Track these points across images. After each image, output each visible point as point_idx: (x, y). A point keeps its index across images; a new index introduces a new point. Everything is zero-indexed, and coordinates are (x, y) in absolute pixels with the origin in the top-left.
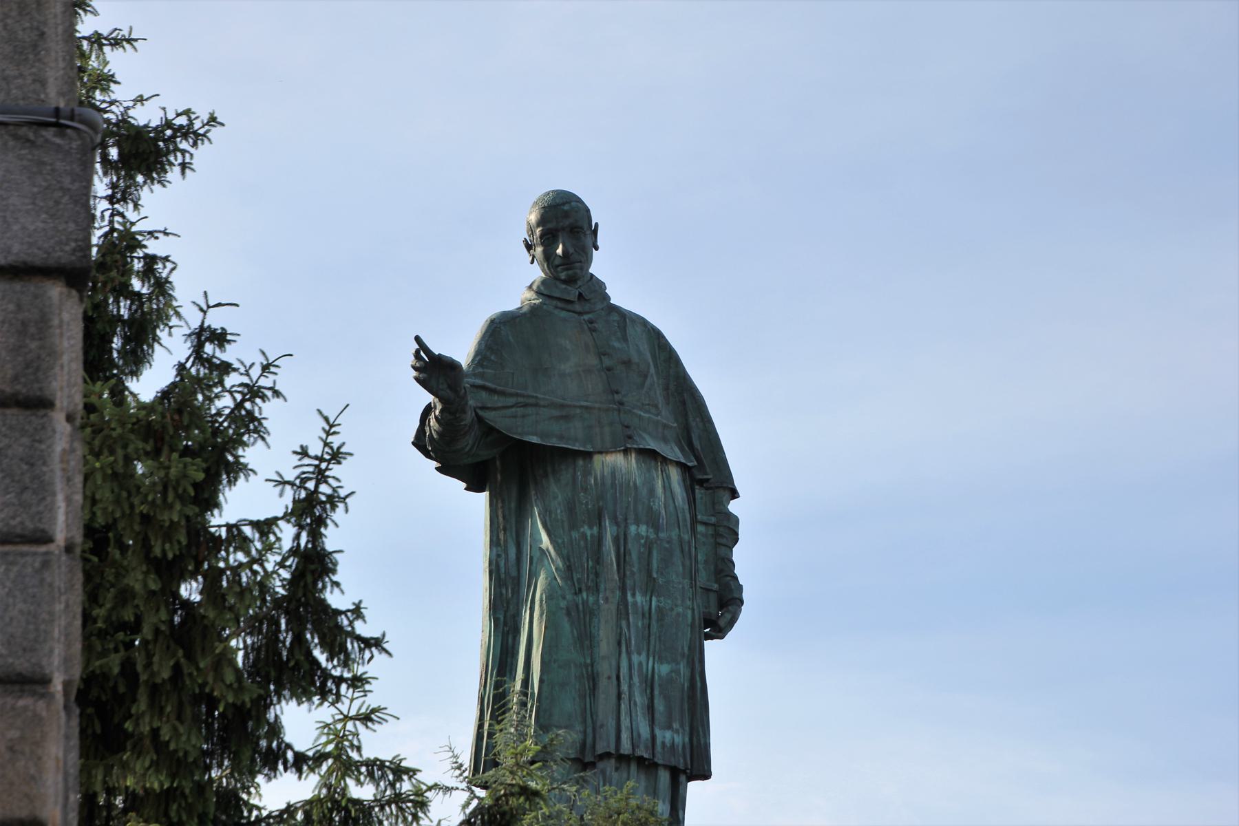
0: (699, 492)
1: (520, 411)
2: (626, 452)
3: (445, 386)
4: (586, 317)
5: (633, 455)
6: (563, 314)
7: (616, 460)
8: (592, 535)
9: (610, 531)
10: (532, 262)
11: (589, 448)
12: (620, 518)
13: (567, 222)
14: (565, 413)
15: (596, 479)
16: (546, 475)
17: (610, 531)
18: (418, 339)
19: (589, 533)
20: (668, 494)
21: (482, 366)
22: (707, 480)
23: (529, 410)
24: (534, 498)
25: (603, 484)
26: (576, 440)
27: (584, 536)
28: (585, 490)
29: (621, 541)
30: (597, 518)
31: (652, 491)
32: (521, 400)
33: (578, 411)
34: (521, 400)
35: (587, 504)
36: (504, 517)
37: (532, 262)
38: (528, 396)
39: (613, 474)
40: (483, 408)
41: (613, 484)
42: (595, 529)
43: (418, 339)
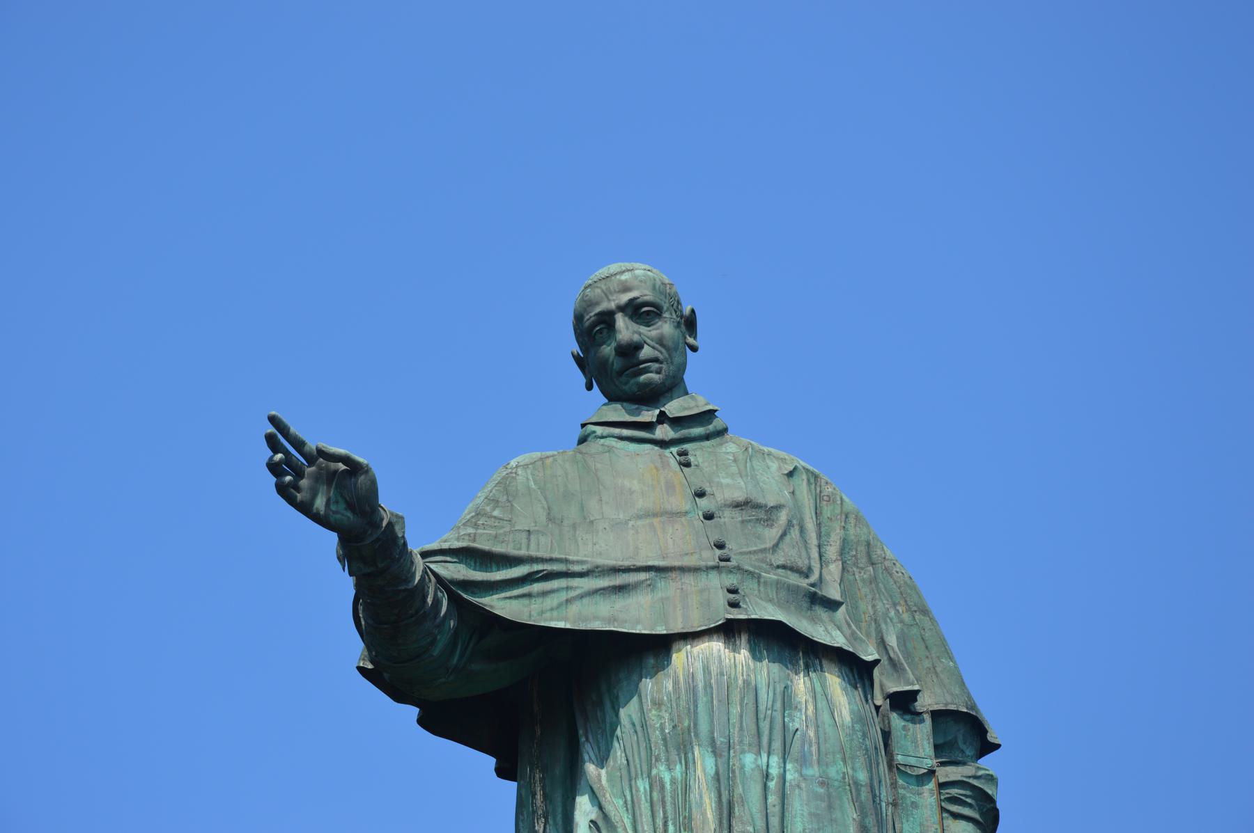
0: (896, 721)
1: (537, 587)
2: (729, 630)
3: (342, 506)
4: (674, 450)
5: (744, 638)
6: (633, 447)
7: (716, 646)
8: (673, 781)
9: (705, 763)
10: (589, 387)
11: (661, 630)
12: (720, 740)
13: (625, 298)
14: (621, 579)
15: (676, 683)
16: (600, 703)
17: (705, 763)
18: (273, 420)
19: (667, 778)
20: (822, 704)
21: (476, 526)
22: (913, 695)
23: (555, 584)
24: (583, 739)
25: (693, 690)
26: (638, 622)
27: (656, 784)
28: (658, 704)
29: (724, 782)
30: (682, 745)
31: (787, 700)
32: (536, 567)
33: (643, 576)
34: (536, 567)
35: (662, 729)
36: (545, 796)
37: (589, 387)
38: (551, 560)
39: (706, 670)
40: (468, 585)
41: (708, 686)
42: (678, 770)
43: (273, 420)
